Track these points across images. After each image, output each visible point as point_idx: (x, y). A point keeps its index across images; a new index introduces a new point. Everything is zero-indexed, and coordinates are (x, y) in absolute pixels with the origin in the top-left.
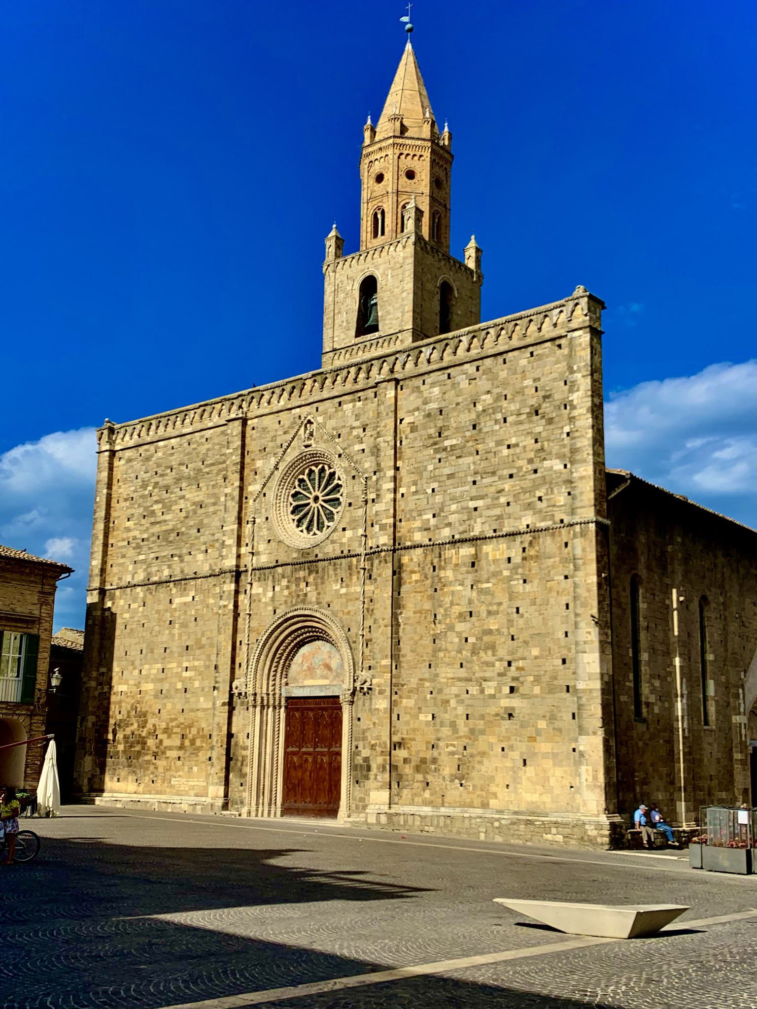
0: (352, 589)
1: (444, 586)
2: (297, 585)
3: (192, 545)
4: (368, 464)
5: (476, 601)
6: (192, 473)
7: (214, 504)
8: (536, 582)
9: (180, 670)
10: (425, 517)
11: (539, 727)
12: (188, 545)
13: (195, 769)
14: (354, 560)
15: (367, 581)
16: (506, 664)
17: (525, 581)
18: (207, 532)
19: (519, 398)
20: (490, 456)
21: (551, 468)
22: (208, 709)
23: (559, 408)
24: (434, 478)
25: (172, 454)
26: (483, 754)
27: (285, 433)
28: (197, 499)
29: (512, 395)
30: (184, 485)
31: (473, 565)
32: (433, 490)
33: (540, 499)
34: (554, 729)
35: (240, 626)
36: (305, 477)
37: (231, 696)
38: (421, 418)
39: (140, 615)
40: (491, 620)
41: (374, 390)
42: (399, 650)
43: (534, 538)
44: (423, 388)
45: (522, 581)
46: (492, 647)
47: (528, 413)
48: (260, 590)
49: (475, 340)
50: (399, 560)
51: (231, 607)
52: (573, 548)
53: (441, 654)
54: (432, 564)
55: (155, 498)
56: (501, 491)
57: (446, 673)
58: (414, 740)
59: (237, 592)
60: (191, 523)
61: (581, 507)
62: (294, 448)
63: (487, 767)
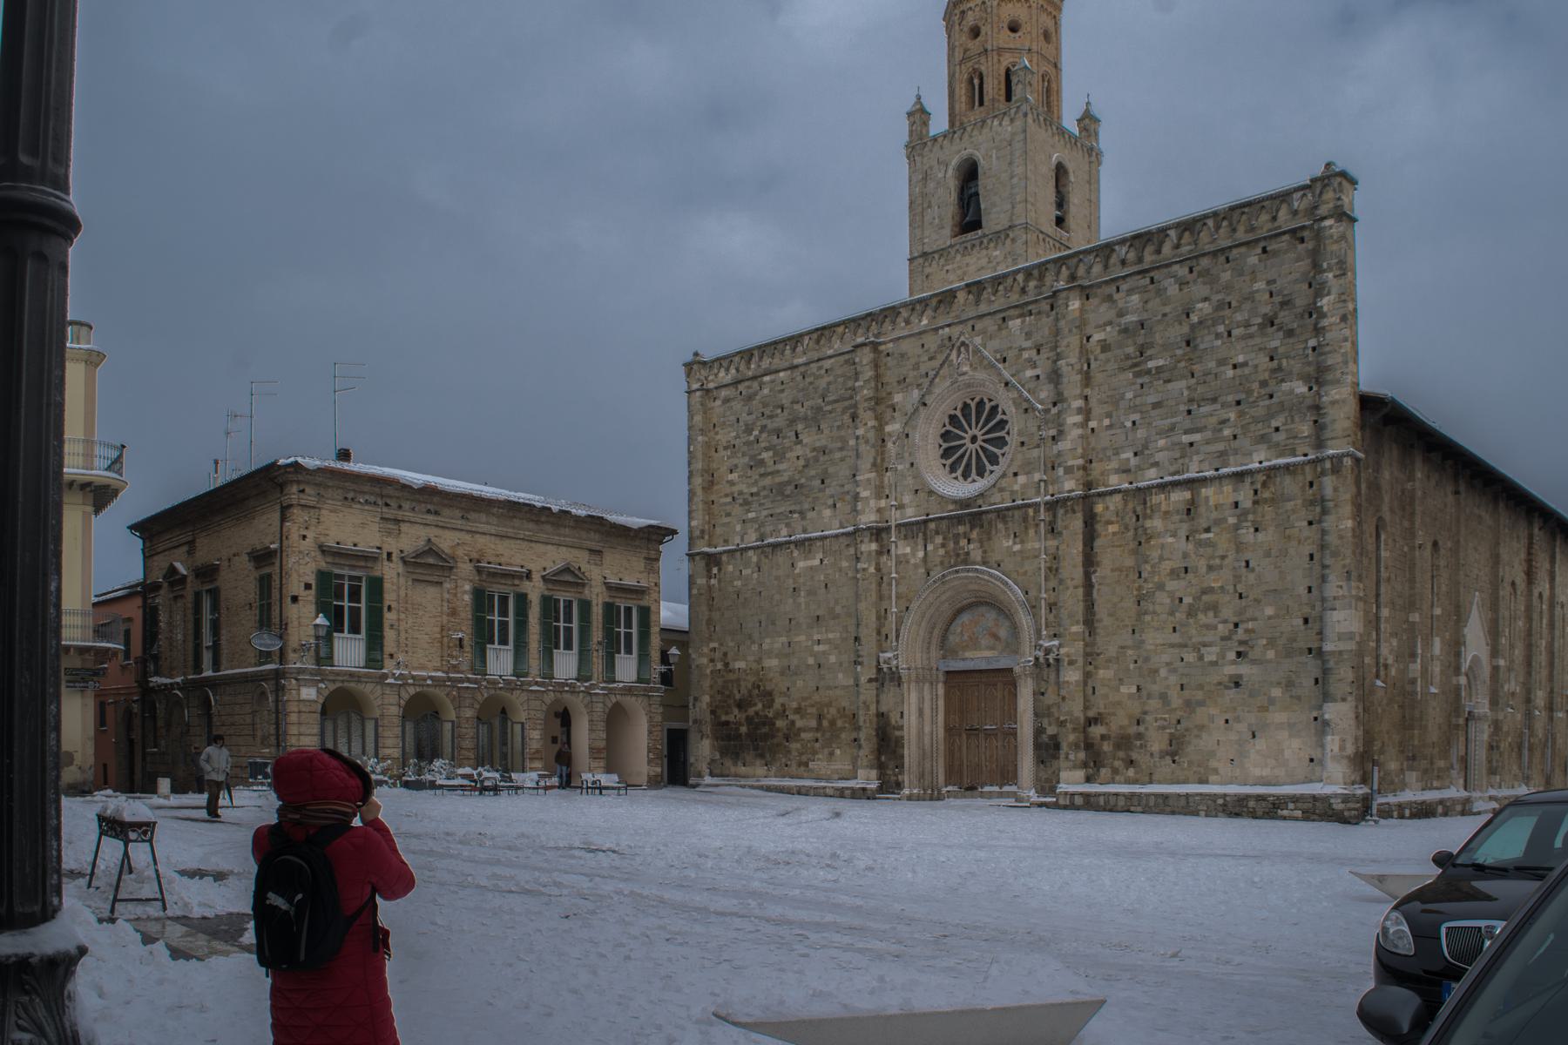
0: (1029, 546)
1: (1151, 538)
2: (956, 543)
3: (816, 499)
4: (1045, 393)
5: (1193, 556)
6: (809, 412)
7: (841, 449)
8: (1271, 530)
9: (810, 643)
10: (1124, 456)
11: (1273, 695)
12: (810, 499)
13: (838, 752)
14: (1031, 512)
15: (1049, 535)
16: (1231, 626)
17: (1257, 530)
18: (835, 483)
19: (1247, 306)
20: (1209, 378)
21: (1292, 391)
22: (848, 687)
23: (1302, 316)
24: (1133, 408)
25: (783, 391)
26: (1201, 728)
27: (931, 359)
28: (818, 444)
29: (1238, 301)
30: (800, 427)
31: (1189, 510)
32: (1134, 423)
33: (1277, 429)
34: (1291, 697)
35: (885, 593)
36: (958, 413)
37: (879, 670)
38: (1115, 334)
39: (755, 582)
40: (1213, 576)
41: (1049, 301)
42: (1093, 614)
43: (1269, 477)
44: (1116, 296)
45: (1252, 530)
46: (1214, 608)
47: (1259, 324)
48: (908, 550)
49: (1187, 234)
50: (1091, 509)
51: (872, 570)
52: (1321, 488)
53: (1148, 618)
54: (1135, 512)
55: (763, 445)
56: (1224, 422)
57: (1153, 638)
58: (1114, 714)
59: (879, 553)
60: (813, 473)
61: (1332, 438)
62: (945, 377)
63: (1206, 741)
